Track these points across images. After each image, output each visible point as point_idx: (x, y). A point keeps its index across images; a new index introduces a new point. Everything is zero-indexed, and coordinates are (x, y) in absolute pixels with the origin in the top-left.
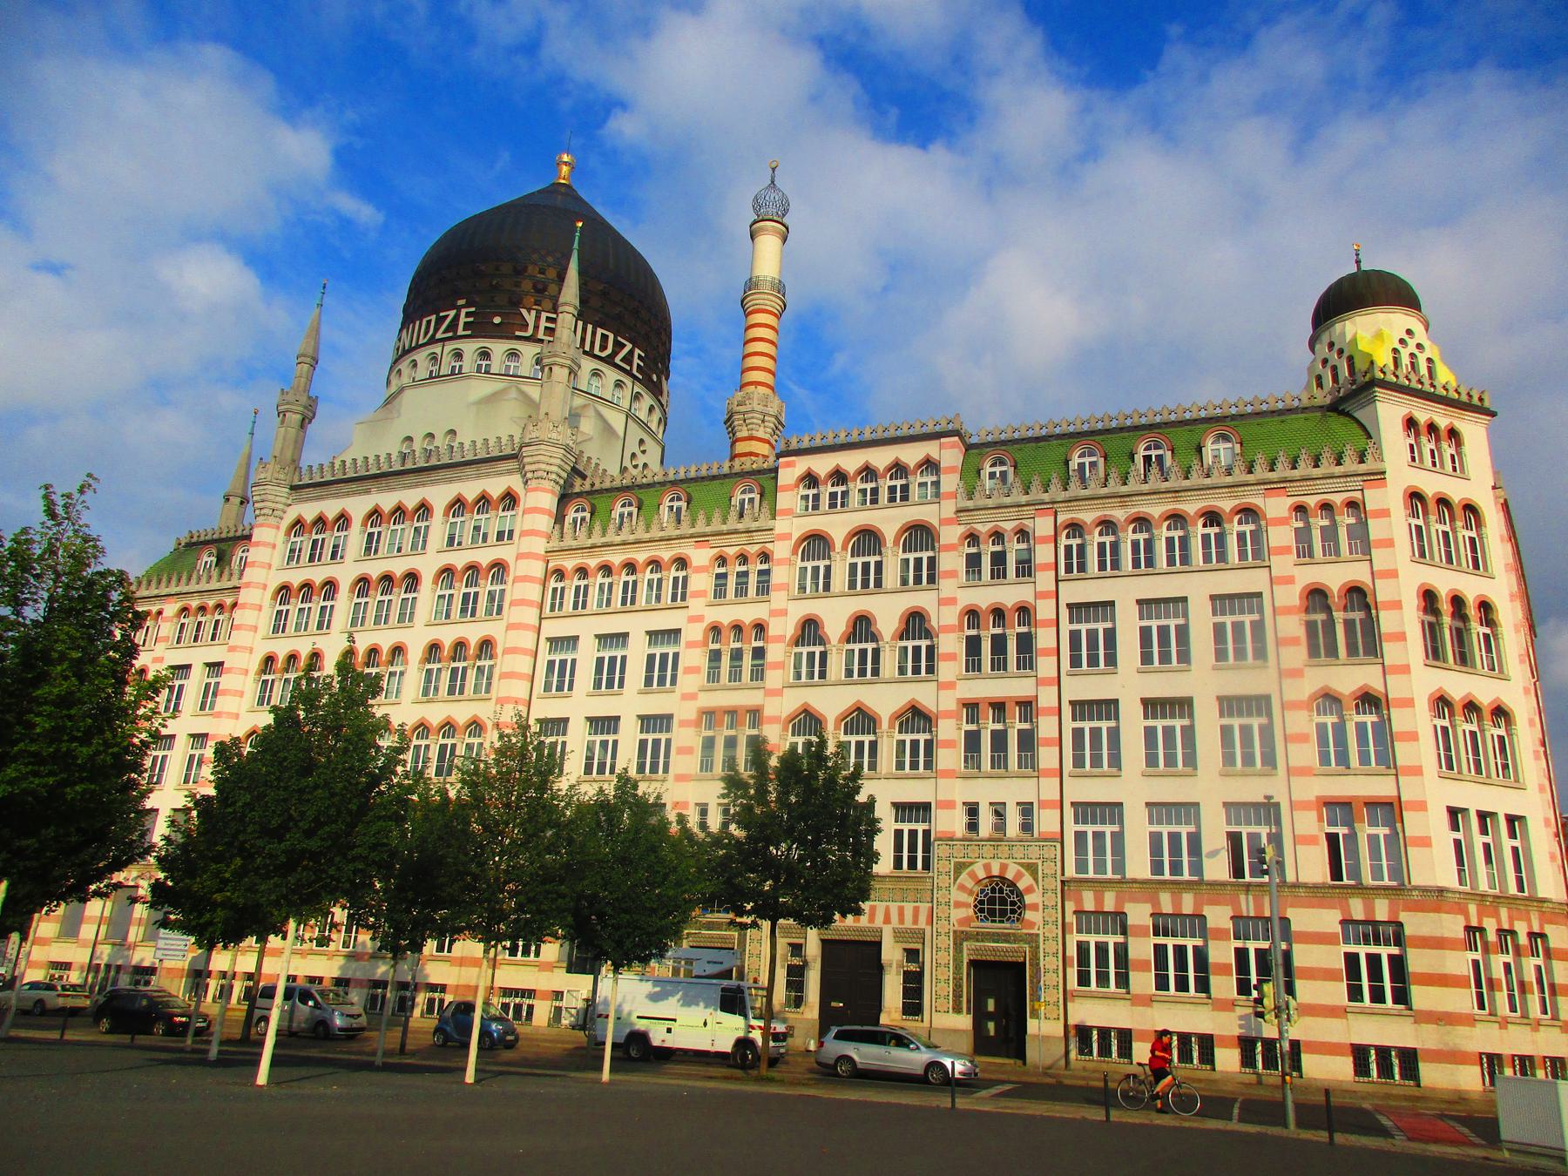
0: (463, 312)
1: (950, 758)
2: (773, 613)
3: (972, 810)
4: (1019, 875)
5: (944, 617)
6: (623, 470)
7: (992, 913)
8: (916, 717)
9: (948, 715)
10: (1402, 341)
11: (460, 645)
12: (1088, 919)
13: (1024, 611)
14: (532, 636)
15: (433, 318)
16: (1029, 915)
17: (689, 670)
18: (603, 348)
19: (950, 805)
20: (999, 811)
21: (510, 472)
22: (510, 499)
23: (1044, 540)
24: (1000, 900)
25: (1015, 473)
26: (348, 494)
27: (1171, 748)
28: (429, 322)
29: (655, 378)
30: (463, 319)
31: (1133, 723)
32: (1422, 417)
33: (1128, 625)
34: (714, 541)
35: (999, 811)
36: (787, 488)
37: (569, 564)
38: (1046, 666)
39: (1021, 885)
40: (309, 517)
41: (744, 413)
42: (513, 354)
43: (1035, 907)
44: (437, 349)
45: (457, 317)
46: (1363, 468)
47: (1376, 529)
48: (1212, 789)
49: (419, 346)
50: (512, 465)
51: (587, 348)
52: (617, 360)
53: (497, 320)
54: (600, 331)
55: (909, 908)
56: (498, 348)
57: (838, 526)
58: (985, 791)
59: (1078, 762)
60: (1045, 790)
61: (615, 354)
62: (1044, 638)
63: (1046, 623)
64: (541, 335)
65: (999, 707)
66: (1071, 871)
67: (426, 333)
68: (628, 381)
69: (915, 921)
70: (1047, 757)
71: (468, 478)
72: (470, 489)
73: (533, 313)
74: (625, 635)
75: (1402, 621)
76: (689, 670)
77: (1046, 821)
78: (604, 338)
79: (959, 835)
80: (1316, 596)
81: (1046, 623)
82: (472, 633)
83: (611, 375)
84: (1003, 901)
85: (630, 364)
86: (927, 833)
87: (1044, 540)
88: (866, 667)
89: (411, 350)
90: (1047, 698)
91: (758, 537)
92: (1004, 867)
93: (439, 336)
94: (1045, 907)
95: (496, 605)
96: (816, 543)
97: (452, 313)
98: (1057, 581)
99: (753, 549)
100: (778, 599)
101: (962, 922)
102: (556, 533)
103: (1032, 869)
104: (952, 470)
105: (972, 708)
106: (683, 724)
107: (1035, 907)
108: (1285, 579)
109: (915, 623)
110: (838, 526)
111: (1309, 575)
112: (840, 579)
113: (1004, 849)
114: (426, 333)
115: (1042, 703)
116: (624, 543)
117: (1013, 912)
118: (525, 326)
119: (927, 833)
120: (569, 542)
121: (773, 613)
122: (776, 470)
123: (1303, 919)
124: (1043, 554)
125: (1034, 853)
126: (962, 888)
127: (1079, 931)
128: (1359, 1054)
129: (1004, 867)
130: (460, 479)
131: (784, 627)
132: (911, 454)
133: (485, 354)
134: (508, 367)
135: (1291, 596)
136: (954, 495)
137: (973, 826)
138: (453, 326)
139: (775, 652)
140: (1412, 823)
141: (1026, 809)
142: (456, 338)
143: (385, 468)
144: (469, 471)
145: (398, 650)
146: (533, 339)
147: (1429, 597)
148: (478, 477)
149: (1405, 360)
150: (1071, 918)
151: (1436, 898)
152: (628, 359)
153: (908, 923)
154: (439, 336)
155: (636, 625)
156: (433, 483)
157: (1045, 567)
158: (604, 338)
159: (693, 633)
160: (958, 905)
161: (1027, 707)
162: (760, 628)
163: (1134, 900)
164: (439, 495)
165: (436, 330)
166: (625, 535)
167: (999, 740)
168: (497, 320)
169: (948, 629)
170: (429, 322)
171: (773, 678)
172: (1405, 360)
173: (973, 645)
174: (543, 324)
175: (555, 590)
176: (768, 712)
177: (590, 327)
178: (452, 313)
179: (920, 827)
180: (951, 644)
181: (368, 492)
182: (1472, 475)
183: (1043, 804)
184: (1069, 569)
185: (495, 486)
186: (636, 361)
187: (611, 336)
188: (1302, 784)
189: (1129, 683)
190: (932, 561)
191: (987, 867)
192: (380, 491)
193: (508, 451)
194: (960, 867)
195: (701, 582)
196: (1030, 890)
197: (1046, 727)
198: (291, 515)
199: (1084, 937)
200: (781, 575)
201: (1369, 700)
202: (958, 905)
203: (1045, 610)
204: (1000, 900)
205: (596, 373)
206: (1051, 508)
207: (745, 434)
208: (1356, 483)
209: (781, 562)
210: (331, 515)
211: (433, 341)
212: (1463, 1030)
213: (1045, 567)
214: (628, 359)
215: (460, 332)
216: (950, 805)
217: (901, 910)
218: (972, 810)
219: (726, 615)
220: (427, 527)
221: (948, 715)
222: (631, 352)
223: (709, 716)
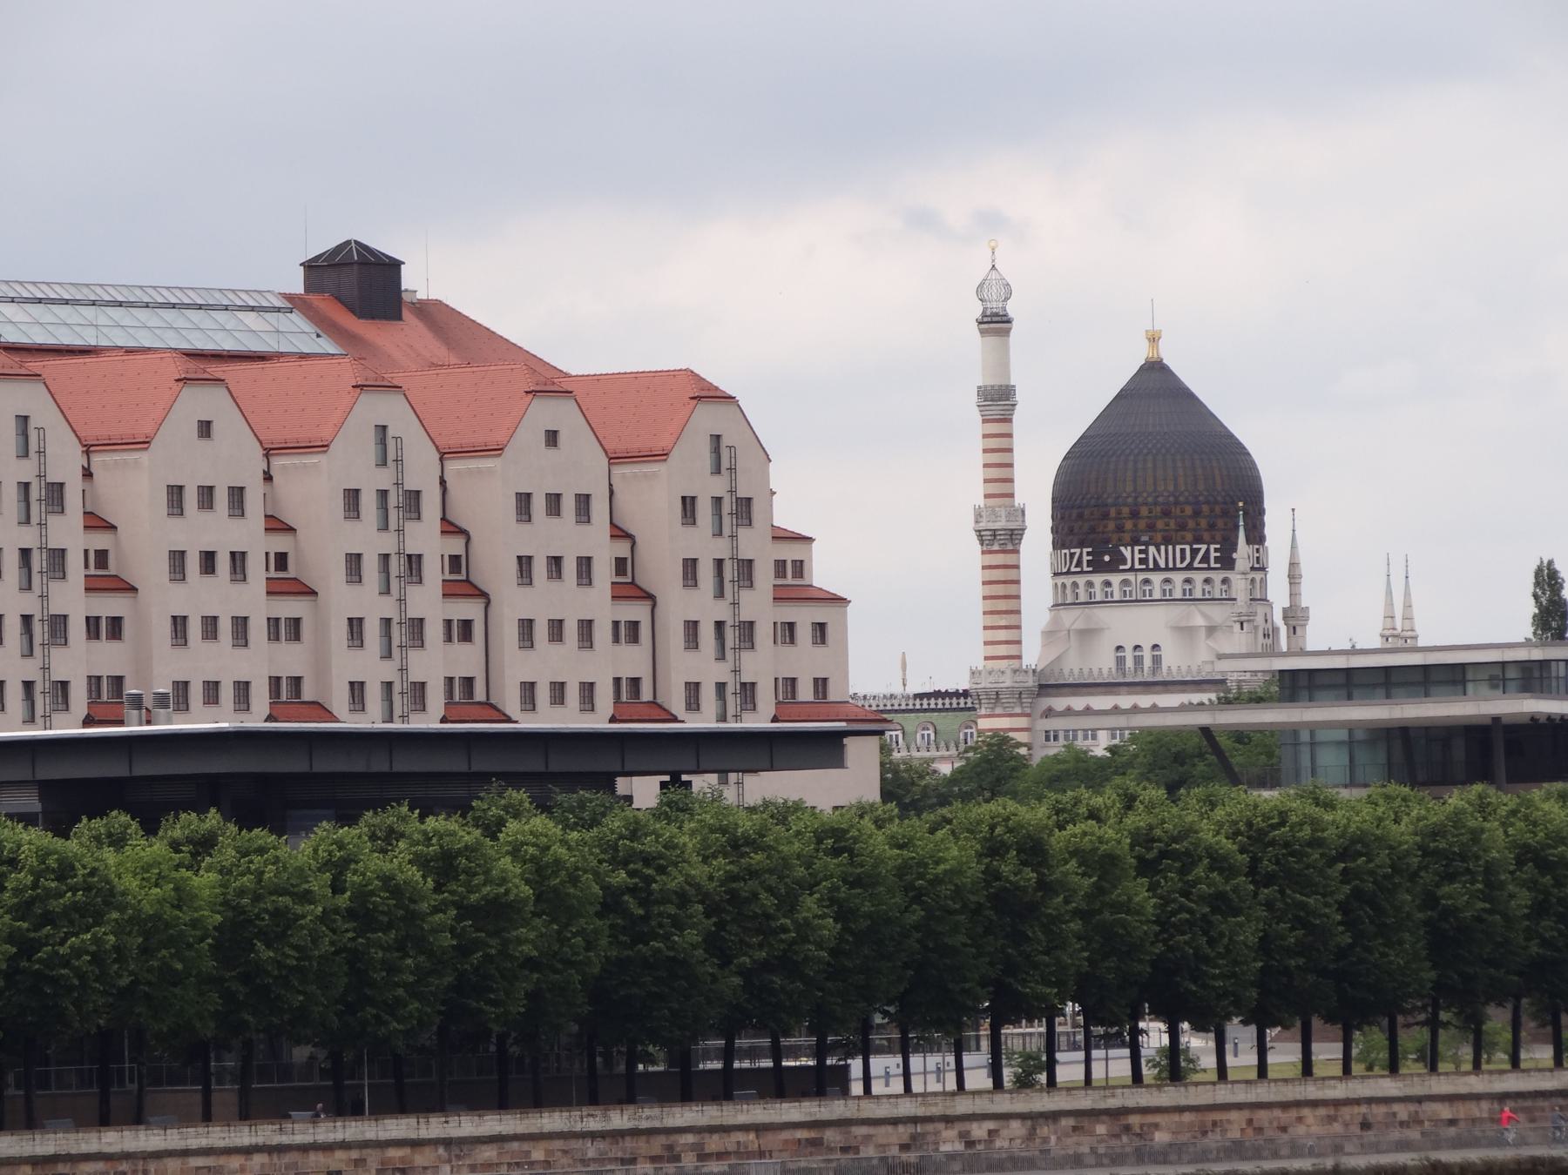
15: (1187, 548)
28: (1183, 551)
30: (1213, 555)
45: (1208, 551)
49: (1175, 569)
89: (1167, 569)
97: (1204, 547)
138: (1206, 559)
142: (1209, 568)
154: (1196, 565)
170: (1183, 551)
178: (1204, 547)
211: (1190, 567)
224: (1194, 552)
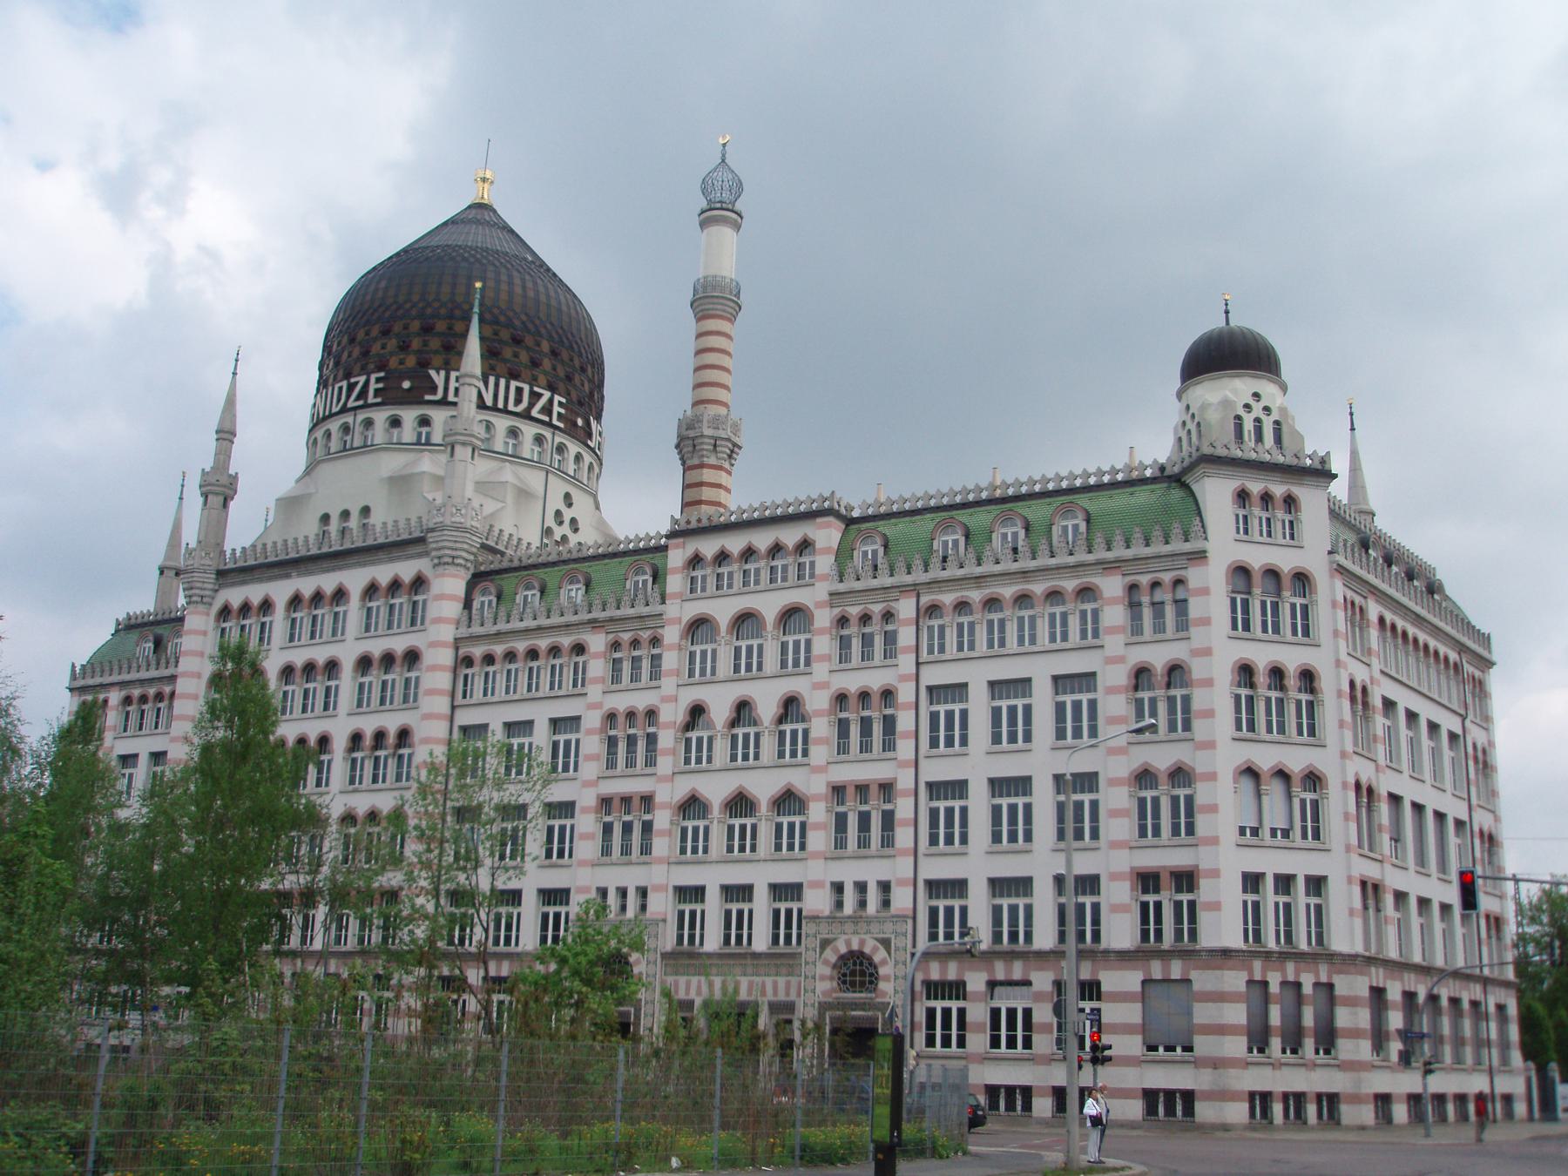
0: (373, 377)
1: (819, 840)
2: (665, 699)
3: (838, 888)
4: (875, 949)
5: (817, 702)
6: (548, 532)
7: (853, 984)
8: (788, 801)
9: (817, 798)
10: (1247, 406)
11: (380, 736)
12: (936, 989)
13: (888, 694)
14: (445, 725)
15: (344, 384)
16: (882, 985)
17: (589, 758)
18: (518, 401)
19: (817, 884)
20: (861, 887)
21: (420, 555)
22: (419, 583)
23: (906, 622)
24: (857, 971)
25: (885, 553)
26: (270, 579)
27: (1011, 828)
29: (580, 422)
30: (373, 386)
31: (979, 803)
32: (1255, 487)
33: (979, 705)
34: (611, 628)
35: (861, 887)
36: (675, 570)
37: (478, 651)
38: (905, 749)
39: (877, 959)
40: (236, 603)
41: (693, 439)
42: (425, 421)
43: (887, 978)
44: (349, 418)
45: (367, 384)
46: (1188, 547)
47: (1195, 609)
48: (1042, 860)
49: (332, 415)
50: (419, 549)
51: (501, 405)
52: (535, 413)
53: (406, 385)
54: (514, 384)
55: (781, 981)
56: (409, 415)
57: (723, 610)
58: (848, 872)
59: (934, 840)
60: (899, 868)
61: (531, 405)
62: (905, 721)
63: (906, 706)
64: (451, 398)
65: (862, 789)
66: (923, 943)
67: (339, 400)
68: (547, 433)
69: (788, 994)
70: (903, 837)
71: (380, 562)
72: (383, 573)
73: (443, 373)
74: (530, 723)
75: (1216, 698)
76: (589, 758)
77: (901, 899)
78: (519, 391)
79: (827, 913)
80: (1141, 675)
81: (906, 706)
82: (392, 722)
83: (529, 430)
84: (863, 973)
85: (550, 414)
86: (800, 911)
87: (906, 622)
88: (744, 753)
89: (325, 418)
90: (905, 780)
91: (651, 623)
92: (862, 942)
93: (351, 404)
94: (896, 978)
95: (410, 696)
96: (698, 627)
97: (362, 379)
98: (918, 664)
99: (645, 635)
100: (668, 684)
101: (824, 993)
102: (465, 619)
103: (886, 943)
104: (827, 551)
105: (838, 791)
106: (585, 810)
107: (887, 978)
108: (1113, 659)
109: (791, 707)
110: (723, 610)
111: (1140, 655)
112: (725, 666)
113: (863, 926)
114: (339, 400)
115: (900, 785)
116: (527, 631)
117: (871, 982)
118: (434, 389)
119: (800, 911)
120: (476, 629)
121: (665, 699)
122: (665, 548)
123: (1110, 980)
124: (906, 636)
125: (888, 930)
126: (826, 962)
127: (928, 998)
128: (1150, 1096)
129: (862, 942)
130: (373, 563)
131: (673, 714)
132: (790, 536)
133: (395, 422)
134: (420, 435)
135: (1117, 676)
136: (825, 578)
137: (839, 904)
138: (363, 394)
139: (666, 739)
140: (1206, 890)
141: (885, 887)
142: (366, 406)
143: (303, 553)
144: (381, 555)
145: (324, 741)
146: (443, 402)
147: (1246, 672)
148: (391, 560)
149: (1248, 425)
150: (918, 987)
151: (1225, 955)
152: (547, 410)
153: (781, 997)
155: (541, 714)
156: (347, 567)
157: (906, 650)
158: (519, 391)
159: (592, 720)
160: (823, 978)
161: (887, 788)
162: (651, 714)
163: (971, 969)
164: (355, 579)
165: (348, 397)
166: (529, 623)
167: (864, 820)
168: (406, 385)
169: (819, 713)
171: (665, 764)
172: (1248, 425)
173: (843, 728)
174: (453, 385)
175: (466, 676)
176: (658, 799)
177: (503, 382)
178: (362, 379)
179: (795, 906)
180: (821, 728)
181: (288, 576)
182: (1305, 544)
183: (902, 882)
184: (931, 652)
185: (405, 570)
186: (556, 409)
187: (526, 388)
188: (1115, 857)
189: (977, 764)
190: (808, 642)
191: (848, 943)
192: (299, 575)
193: (417, 534)
194: (825, 944)
195: (597, 668)
196: (884, 962)
197: (903, 808)
198: (218, 605)
199: (932, 1003)
200: (670, 660)
201: (1180, 775)
202: (823, 978)
203: (906, 693)
204: (857, 971)
205: (513, 433)
206: (915, 589)
207: (696, 461)
208: (1182, 562)
209: (671, 647)
210: (256, 601)
211: (344, 410)
212: (1233, 1072)
213: (906, 650)
214: (547, 410)
215: (371, 400)
216: (817, 884)
217: (775, 984)
218: (838, 888)
219: (621, 703)
220: (345, 613)
221: (817, 798)
222: (551, 401)
223: (606, 803)
224: (351, 387)
